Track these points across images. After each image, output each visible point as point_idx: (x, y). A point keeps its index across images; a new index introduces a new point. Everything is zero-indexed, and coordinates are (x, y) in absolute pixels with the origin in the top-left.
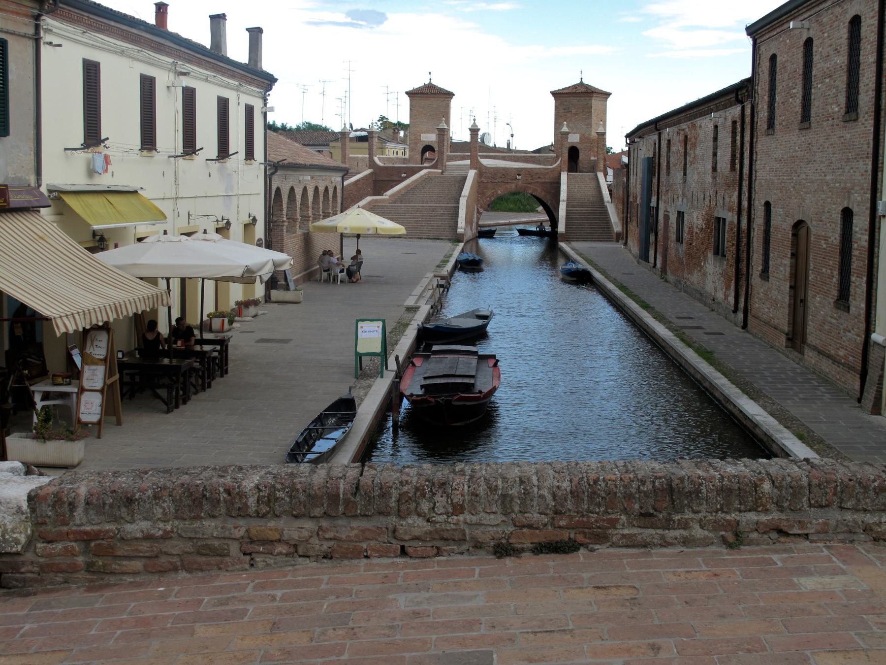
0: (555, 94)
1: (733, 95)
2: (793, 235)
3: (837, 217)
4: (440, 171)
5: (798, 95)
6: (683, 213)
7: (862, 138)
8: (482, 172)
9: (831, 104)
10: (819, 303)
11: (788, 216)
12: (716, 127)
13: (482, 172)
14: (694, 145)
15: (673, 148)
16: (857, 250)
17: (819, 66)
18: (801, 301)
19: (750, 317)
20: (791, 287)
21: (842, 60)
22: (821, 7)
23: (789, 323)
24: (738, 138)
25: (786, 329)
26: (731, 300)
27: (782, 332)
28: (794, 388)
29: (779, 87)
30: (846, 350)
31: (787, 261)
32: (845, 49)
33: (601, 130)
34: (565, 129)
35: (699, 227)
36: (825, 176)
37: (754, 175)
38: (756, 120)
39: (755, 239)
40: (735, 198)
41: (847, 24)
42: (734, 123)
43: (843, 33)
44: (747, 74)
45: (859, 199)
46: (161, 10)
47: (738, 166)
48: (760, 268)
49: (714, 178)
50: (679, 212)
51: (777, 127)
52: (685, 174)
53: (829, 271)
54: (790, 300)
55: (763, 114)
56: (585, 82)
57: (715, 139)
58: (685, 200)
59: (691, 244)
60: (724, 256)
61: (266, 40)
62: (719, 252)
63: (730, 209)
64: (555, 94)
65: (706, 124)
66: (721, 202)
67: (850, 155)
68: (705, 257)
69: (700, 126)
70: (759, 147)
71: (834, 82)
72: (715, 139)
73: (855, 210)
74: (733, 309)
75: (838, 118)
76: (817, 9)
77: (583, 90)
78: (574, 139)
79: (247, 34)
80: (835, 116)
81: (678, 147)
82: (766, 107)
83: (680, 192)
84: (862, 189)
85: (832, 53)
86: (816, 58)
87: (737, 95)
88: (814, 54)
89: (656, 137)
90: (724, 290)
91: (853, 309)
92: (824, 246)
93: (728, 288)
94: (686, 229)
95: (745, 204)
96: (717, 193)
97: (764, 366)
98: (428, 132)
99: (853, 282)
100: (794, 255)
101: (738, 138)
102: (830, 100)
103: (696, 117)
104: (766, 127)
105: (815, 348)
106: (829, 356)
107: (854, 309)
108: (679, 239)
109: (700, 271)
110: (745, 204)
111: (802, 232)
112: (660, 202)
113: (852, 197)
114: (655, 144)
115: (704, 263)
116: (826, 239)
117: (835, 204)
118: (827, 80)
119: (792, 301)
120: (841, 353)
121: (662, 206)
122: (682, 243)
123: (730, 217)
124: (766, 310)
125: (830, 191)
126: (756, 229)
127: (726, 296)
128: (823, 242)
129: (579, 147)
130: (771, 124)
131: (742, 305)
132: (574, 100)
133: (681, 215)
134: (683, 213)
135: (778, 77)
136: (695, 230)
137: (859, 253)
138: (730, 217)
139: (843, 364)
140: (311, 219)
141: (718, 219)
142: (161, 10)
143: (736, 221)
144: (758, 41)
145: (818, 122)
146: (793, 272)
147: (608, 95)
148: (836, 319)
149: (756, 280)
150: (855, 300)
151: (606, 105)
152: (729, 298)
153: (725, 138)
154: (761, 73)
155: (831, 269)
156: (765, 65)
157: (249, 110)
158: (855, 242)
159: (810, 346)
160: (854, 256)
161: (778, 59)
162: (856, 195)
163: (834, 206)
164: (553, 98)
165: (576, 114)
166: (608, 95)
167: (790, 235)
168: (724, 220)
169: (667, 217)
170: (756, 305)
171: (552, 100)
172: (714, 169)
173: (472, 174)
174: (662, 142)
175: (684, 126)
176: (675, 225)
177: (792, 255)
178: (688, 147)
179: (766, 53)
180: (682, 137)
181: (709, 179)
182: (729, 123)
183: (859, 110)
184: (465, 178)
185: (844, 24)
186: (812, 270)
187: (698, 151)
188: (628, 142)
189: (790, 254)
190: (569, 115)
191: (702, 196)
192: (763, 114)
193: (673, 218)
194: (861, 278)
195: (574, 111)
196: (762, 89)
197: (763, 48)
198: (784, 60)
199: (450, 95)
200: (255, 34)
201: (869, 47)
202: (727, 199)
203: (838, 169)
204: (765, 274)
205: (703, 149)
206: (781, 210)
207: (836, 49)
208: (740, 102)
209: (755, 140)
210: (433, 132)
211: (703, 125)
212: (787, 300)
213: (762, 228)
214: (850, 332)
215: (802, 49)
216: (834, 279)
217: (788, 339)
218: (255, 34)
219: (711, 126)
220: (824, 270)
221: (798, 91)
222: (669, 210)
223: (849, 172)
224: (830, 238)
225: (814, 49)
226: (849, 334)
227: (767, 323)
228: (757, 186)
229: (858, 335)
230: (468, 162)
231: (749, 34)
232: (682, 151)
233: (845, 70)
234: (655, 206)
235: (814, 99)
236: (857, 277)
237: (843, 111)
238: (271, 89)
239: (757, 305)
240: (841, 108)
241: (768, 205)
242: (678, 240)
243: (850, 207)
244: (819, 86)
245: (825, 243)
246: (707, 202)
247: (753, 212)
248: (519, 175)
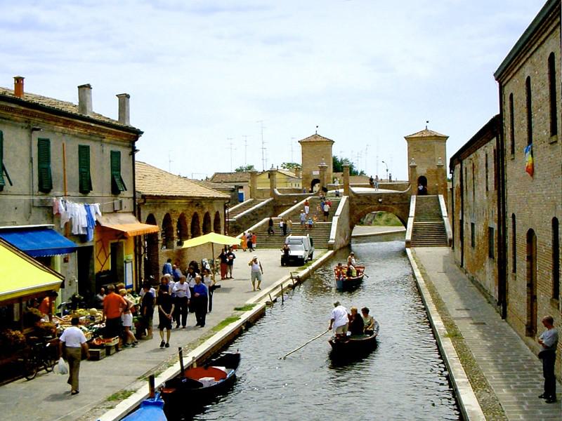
3: (550, 225)
12: (487, 155)
15: (468, 174)
20: (528, 285)
23: (528, 316)
28: (517, 375)
33: (440, 163)
42: (495, 150)
46: (19, 81)
49: (487, 196)
51: (516, 151)
54: (528, 296)
56: (429, 128)
60: (493, 258)
61: (132, 103)
77: (428, 135)
78: (421, 171)
79: (118, 98)
80: (545, 140)
81: (470, 174)
94: (476, 237)
97: (502, 353)
119: (530, 297)
123: (495, 226)
132: (421, 142)
135: (515, 111)
136: (480, 238)
142: (19, 81)
146: (529, 272)
147: (448, 137)
149: (510, 279)
151: (445, 145)
157: (115, 156)
164: (406, 141)
165: (424, 152)
173: (344, 199)
181: (485, 198)
184: (338, 203)
190: (418, 153)
192: (508, 143)
195: (421, 150)
196: (507, 122)
199: (333, 142)
200: (124, 99)
218: (124, 99)
221: (525, 121)
231: (496, 80)
238: (137, 140)
241: (514, 216)
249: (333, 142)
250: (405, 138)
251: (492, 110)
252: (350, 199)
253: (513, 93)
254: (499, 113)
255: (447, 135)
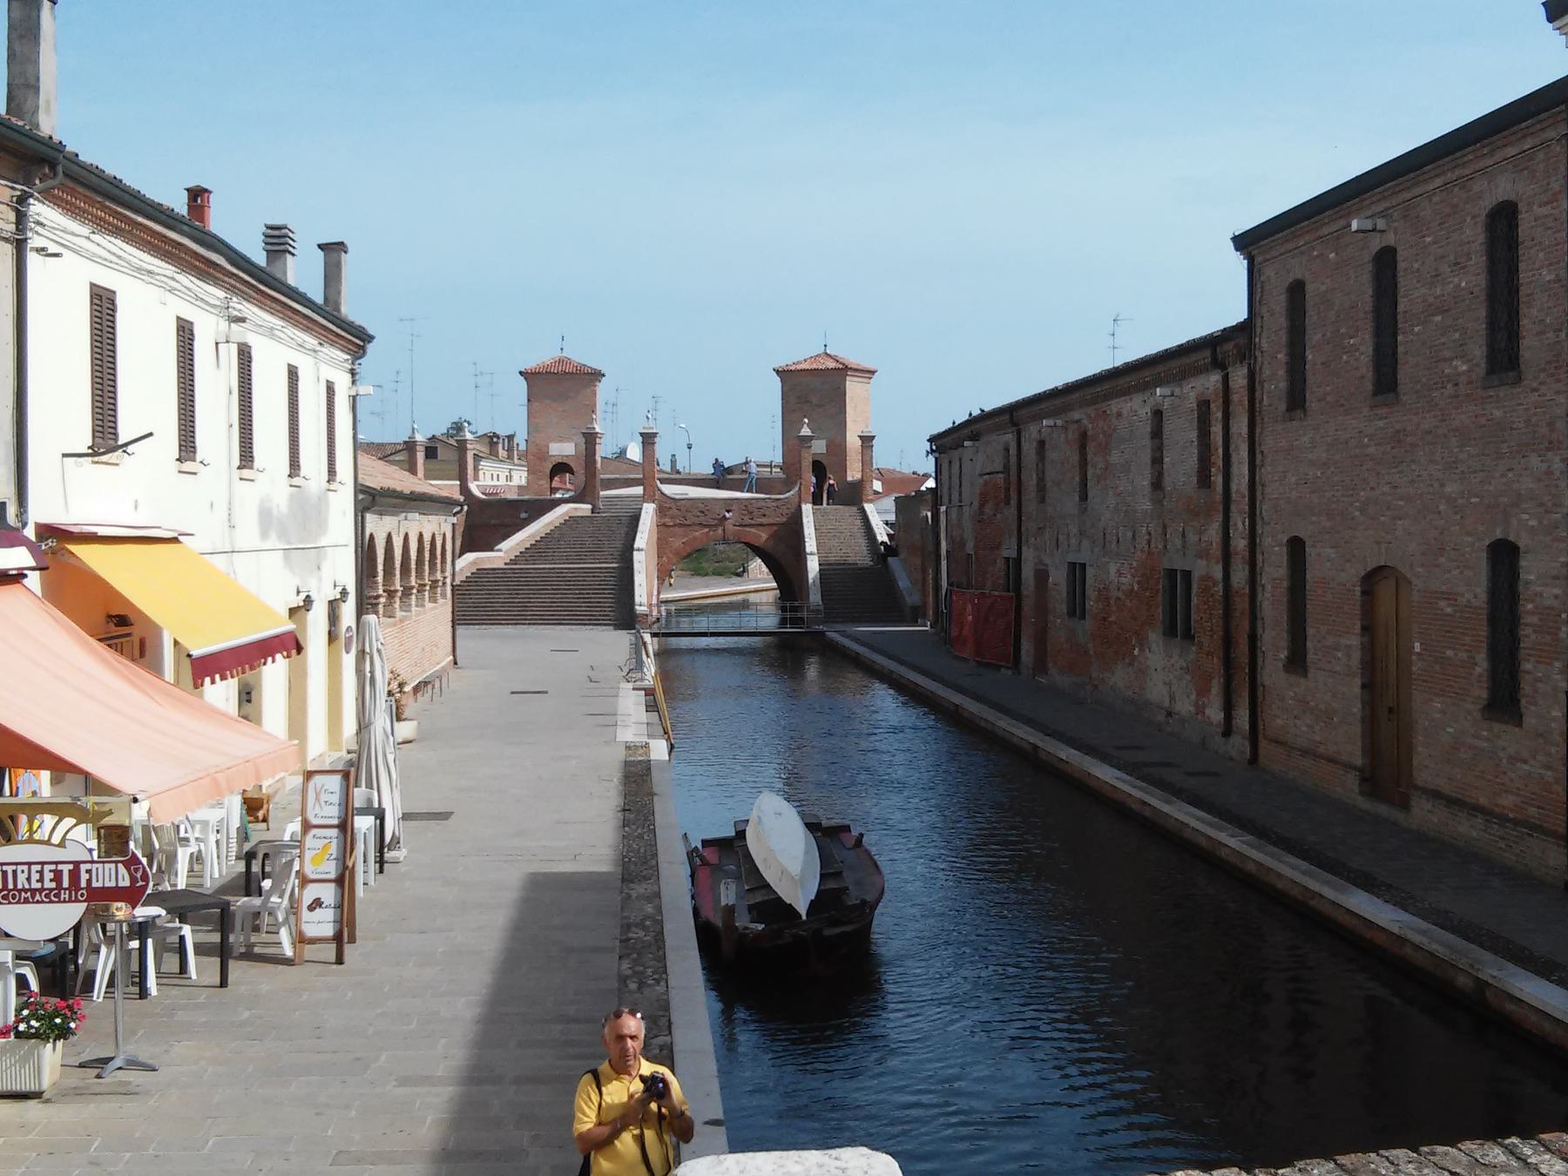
0: (782, 373)
1: (1207, 353)
2: (1364, 593)
4: (590, 506)
5: (1362, 348)
6: (1083, 566)
7: (1535, 414)
8: (667, 507)
9: (1451, 359)
10: (1443, 712)
11: (1348, 561)
12: (1158, 414)
13: (667, 507)
14: (1105, 448)
15: (1052, 455)
16: (1532, 613)
17: (1412, 294)
18: (1391, 710)
19: (1263, 745)
20: (1364, 686)
21: (1472, 279)
22: (1417, 191)
24: (1217, 430)
25: (1359, 762)
26: (1215, 714)
27: (1349, 766)
29: (1314, 337)
30: (1518, 795)
31: (1354, 641)
32: (1478, 260)
34: (806, 431)
35: (1123, 588)
36: (1443, 485)
37: (1258, 493)
38: (1258, 394)
39: (1266, 604)
40: (1214, 532)
41: (1482, 218)
42: (1204, 406)
43: (1474, 235)
44: (1242, 315)
45: (1533, 523)
47: (1218, 480)
48: (1283, 655)
49: (1158, 502)
50: (1072, 566)
51: (1312, 403)
52: (1084, 497)
53: (1463, 655)
54: (1363, 708)
55: (1275, 382)
57: (1157, 434)
58: (1086, 543)
59: (1104, 619)
60: (1188, 636)
62: (1178, 628)
63: (1203, 554)
64: (782, 373)
65: (1136, 409)
66: (1178, 542)
67: (1505, 445)
68: (1143, 643)
69: (1119, 415)
70: (1269, 441)
71: (1455, 319)
72: (1157, 434)
73: (1523, 542)
74: (1220, 730)
75: (1470, 383)
76: (1407, 195)
77: (831, 365)
81: (1062, 454)
82: (1281, 372)
83: (1074, 530)
84: (1541, 505)
85: (1445, 269)
86: (1403, 282)
87: (1214, 353)
88: (1400, 274)
89: (1010, 437)
90: (1193, 697)
91: (1530, 721)
92: (1449, 610)
93: (1203, 691)
94: (1091, 593)
95: (1240, 543)
96: (1165, 527)
98: (561, 439)
99: (1528, 672)
100: (1367, 629)
101: (1217, 430)
102: (1447, 354)
103: (1107, 397)
104: (1283, 407)
105: (1436, 795)
106: (1476, 809)
107: (1534, 721)
108: (1077, 608)
109: (1131, 664)
110: (1240, 543)
111: (1385, 590)
112: (1024, 549)
113: (1514, 522)
114: (1007, 450)
115: (1142, 650)
116: (1450, 597)
117: (1469, 534)
118: (1438, 318)
120: (1508, 801)
121: (1028, 555)
122: (1083, 617)
124: (1304, 729)
125: (1456, 513)
126: (1269, 587)
127: (1200, 710)
128: (1442, 604)
129: (825, 462)
130: (1296, 400)
131: (1242, 718)
133: (1077, 572)
134: (1083, 566)
135: (1312, 317)
136: (1114, 594)
137: (1541, 620)
138: (1207, 569)
139: (1516, 823)
140: (415, 591)
141: (1171, 574)
143: (1218, 572)
144: (1258, 259)
145: (1417, 392)
147: (873, 372)
148: (1488, 740)
150: (1535, 704)
152: (1207, 711)
153: (1182, 435)
154: (1266, 316)
155: (1467, 651)
156: (1278, 302)
158: (1528, 601)
159: (1416, 788)
160: (1527, 625)
161: (1310, 288)
162: (1525, 516)
163: (1470, 539)
165: (820, 406)
166: (873, 372)
167: (1358, 594)
168: (1187, 575)
169: (1042, 576)
170: (1277, 719)
171: (776, 383)
172: (1157, 485)
173: (649, 512)
174: (1025, 446)
175: (1076, 415)
176: (1063, 588)
177: (1364, 629)
178: (1091, 449)
179: (1277, 279)
180: (1072, 435)
181: (1147, 505)
182: (1191, 403)
183: (1522, 367)
184: (635, 520)
185: (1474, 217)
186: (1419, 654)
187: (1115, 457)
188: (934, 448)
189: (1358, 626)
191: (1130, 534)
193: (1058, 577)
194: (1550, 664)
195: (814, 401)
197: (1269, 272)
198: (1323, 288)
199: (597, 375)
201: (1541, 255)
202: (1192, 538)
203: (1475, 472)
204: (1297, 661)
205: (1131, 454)
206: (1330, 551)
207: (1456, 264)
208: (1219, 365)
209: (1258, 430)
210: (568, 440)
211: (1125, 413)
212: (1357, 708)
213: (1285, 584)
214: (1525, 762)
215: (1370, 267)
216: (1478, 670)
217: (1363, 780)
219: (1145, 412)
220: (1449, 653)
222: (1048, 561)
223: (1503, 476)
224: (1463, 595)
225: (1401, 265)
226: (1526, 767)
227: (1305, 752)
228: (1265, 509)
229: (1549, 768)
230: (639, 490)
231: (1237, 249)
232: (1075, 458)
233: (1483, 297)
234: (1014, 555)
235: (1406, 353)
236: (1538, 662)
237: (1481, 370)
239: (1279, 722)
240: (1478, 365)
242: (1072, 613)
243: (1512, 538)
244: (1416, 329)
245: (1449, 605)
246: (1142, 542)
247: (1259, 558)
248: (728, 511)
249: (597, 375)
250: (778, 372)
251: (1237, 313)
252: (661, 511)
253: (1308, 277)
254: (1245, 316)
255: (871, 367)
